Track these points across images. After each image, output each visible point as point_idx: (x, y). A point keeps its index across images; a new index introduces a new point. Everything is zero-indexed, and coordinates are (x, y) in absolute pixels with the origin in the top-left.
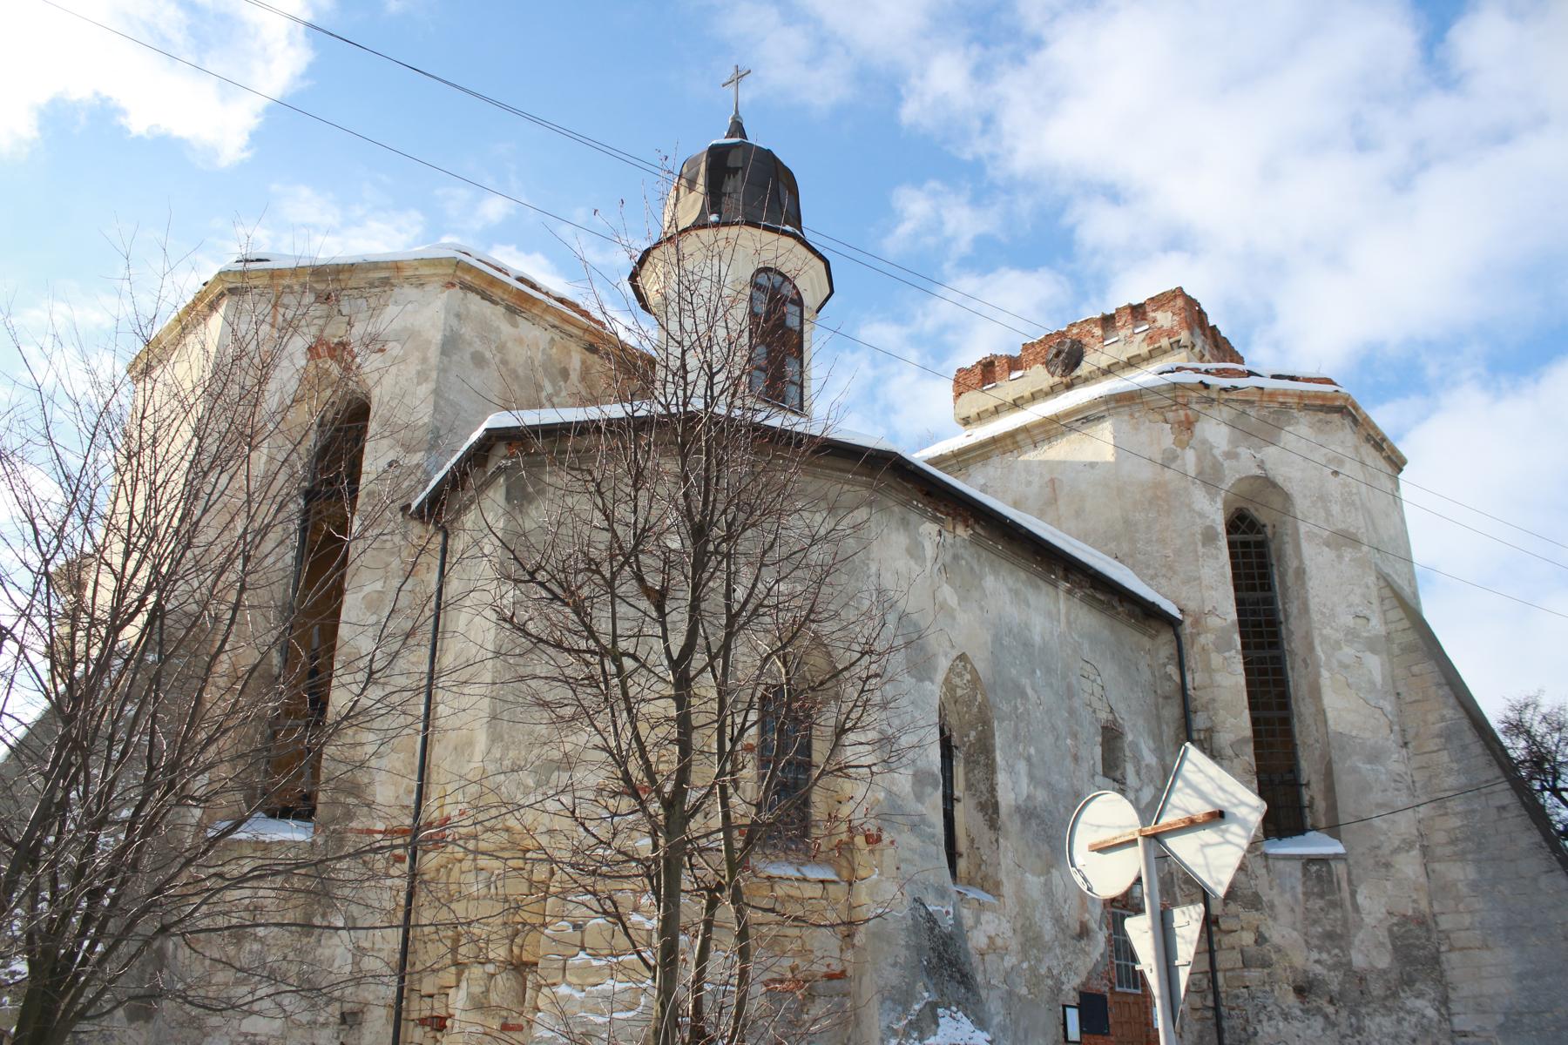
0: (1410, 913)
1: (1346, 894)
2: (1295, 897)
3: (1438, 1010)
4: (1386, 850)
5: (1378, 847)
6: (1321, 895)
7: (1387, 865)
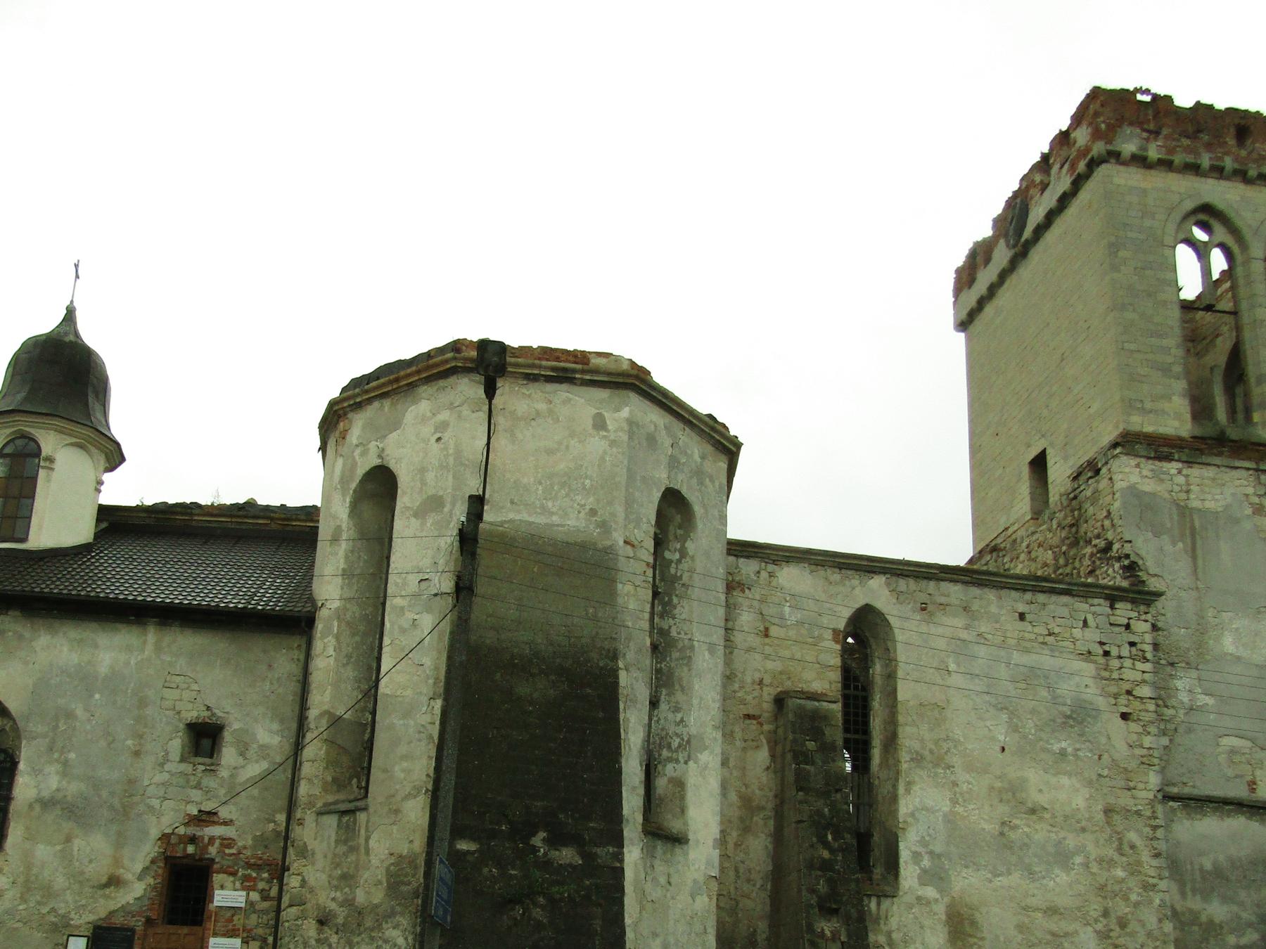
0: (405, 852)
1: (362, 841)
2: (329, 844)
3: (406, 939)
4: (399, 798)
5: (394, 796)
6: (345, 842)
7: (397, 811)
